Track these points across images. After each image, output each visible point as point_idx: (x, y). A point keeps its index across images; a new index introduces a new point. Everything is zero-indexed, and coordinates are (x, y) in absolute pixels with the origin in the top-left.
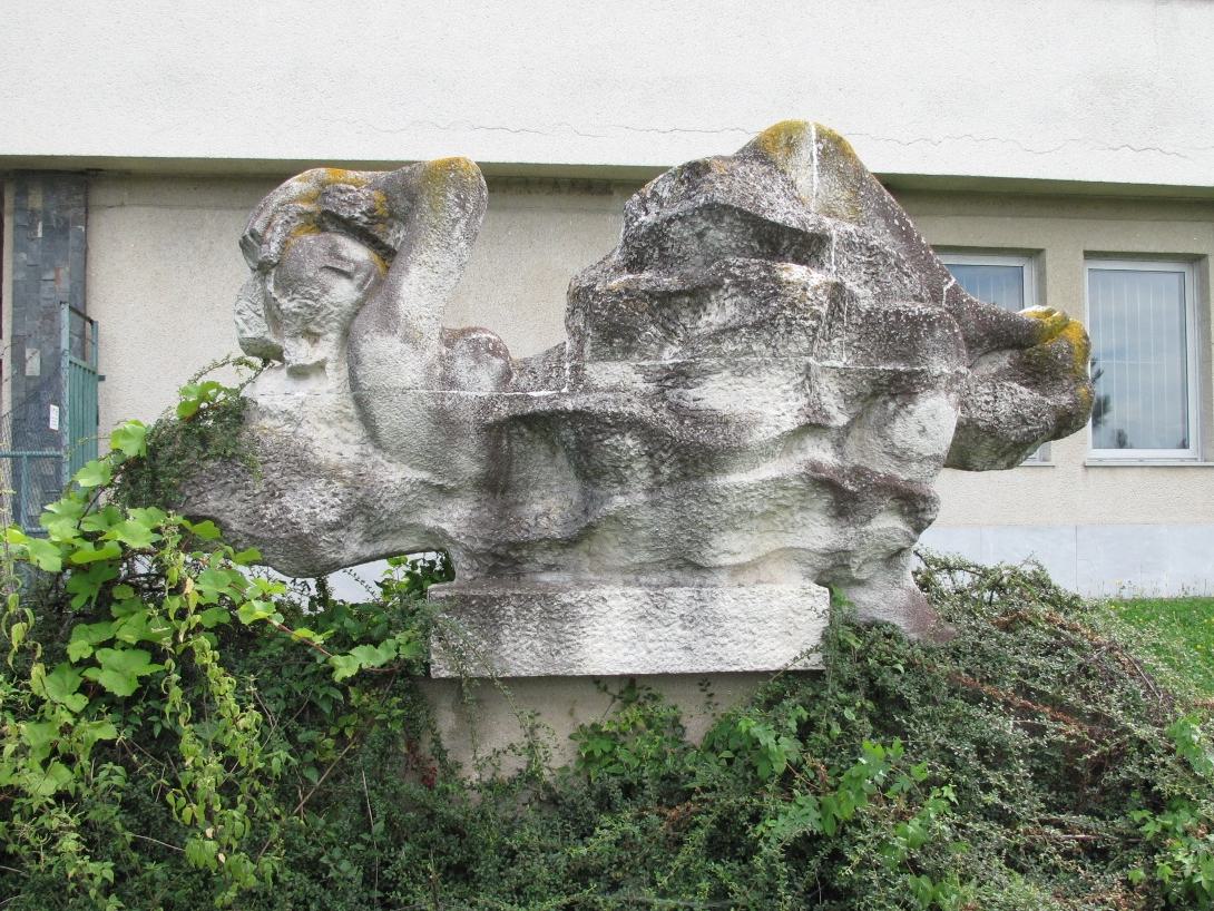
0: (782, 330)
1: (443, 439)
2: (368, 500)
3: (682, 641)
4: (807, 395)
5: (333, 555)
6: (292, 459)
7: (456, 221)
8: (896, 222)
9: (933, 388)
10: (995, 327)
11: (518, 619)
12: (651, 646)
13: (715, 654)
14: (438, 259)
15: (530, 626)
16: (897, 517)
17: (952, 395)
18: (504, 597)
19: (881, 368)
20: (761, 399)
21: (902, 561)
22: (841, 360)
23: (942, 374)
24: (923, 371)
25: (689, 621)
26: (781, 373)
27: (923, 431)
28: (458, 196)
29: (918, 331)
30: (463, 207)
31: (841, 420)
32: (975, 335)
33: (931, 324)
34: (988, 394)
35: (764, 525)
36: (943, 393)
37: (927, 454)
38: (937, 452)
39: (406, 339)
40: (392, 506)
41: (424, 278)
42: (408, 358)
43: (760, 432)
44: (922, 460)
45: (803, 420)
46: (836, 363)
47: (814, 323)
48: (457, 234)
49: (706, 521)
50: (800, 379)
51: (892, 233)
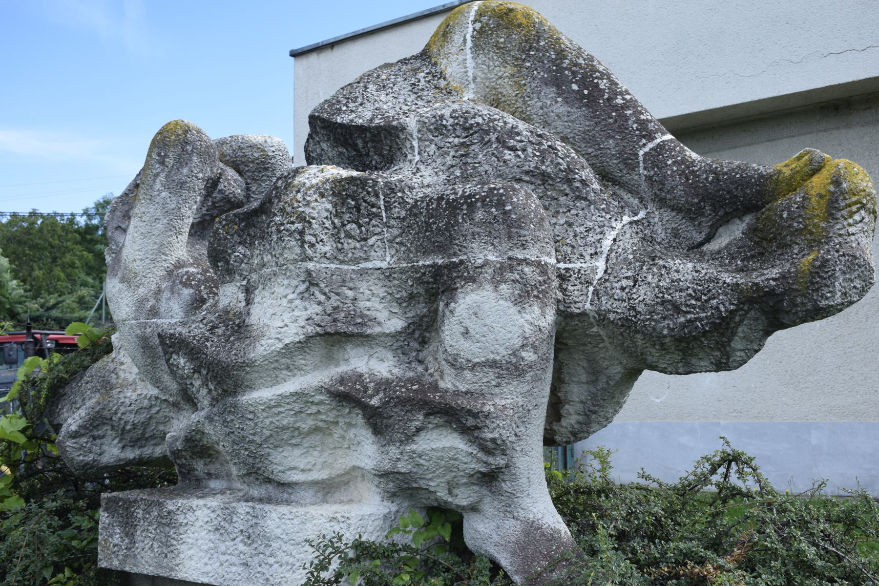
0: (275, 237)
1: (149, 360)
2: (105, 413)
3: (242, 556)
4: (319, 303)
5: (81, 458)
6: (101, 379)
7: (157, 175)
8: (575, 87)
9: (474, 281)
10: (711, 188)
11: (144, 522)
12: (223, 558)
13: (264, 574)
14: (143, 209)
15: (150, 528)
16: (455, 435)
17: (503, 287)
18: (135, 501)
19: (421, 263)
20: (271, 311)
21: (506, 486)
22: (383, 259)
23: (486, 263)
24: (462, 262)
25: (249, 538)
26: (286, 282)
27: (466, 333)
28: (159, 155)
29: (455, 216)
30: (162, 163)
31: (396, 324)
32: (687, 202)
33: (472, 207)
34: (627, 278)
35: (316, 438)
36: (489, 287)
37: (476, 360)
38: (491, 357)
39: (123, 280)
40: (131, 417)
41: (136, 227)
42: (123, 295)
43: (262, 346)
44: (474, 367)
45: (310, 329)
46: (379, 264)
47: (299, 226)
48: (158, 186)
49: (251, 437)
50: (302, 287)
51: (566, 101)
